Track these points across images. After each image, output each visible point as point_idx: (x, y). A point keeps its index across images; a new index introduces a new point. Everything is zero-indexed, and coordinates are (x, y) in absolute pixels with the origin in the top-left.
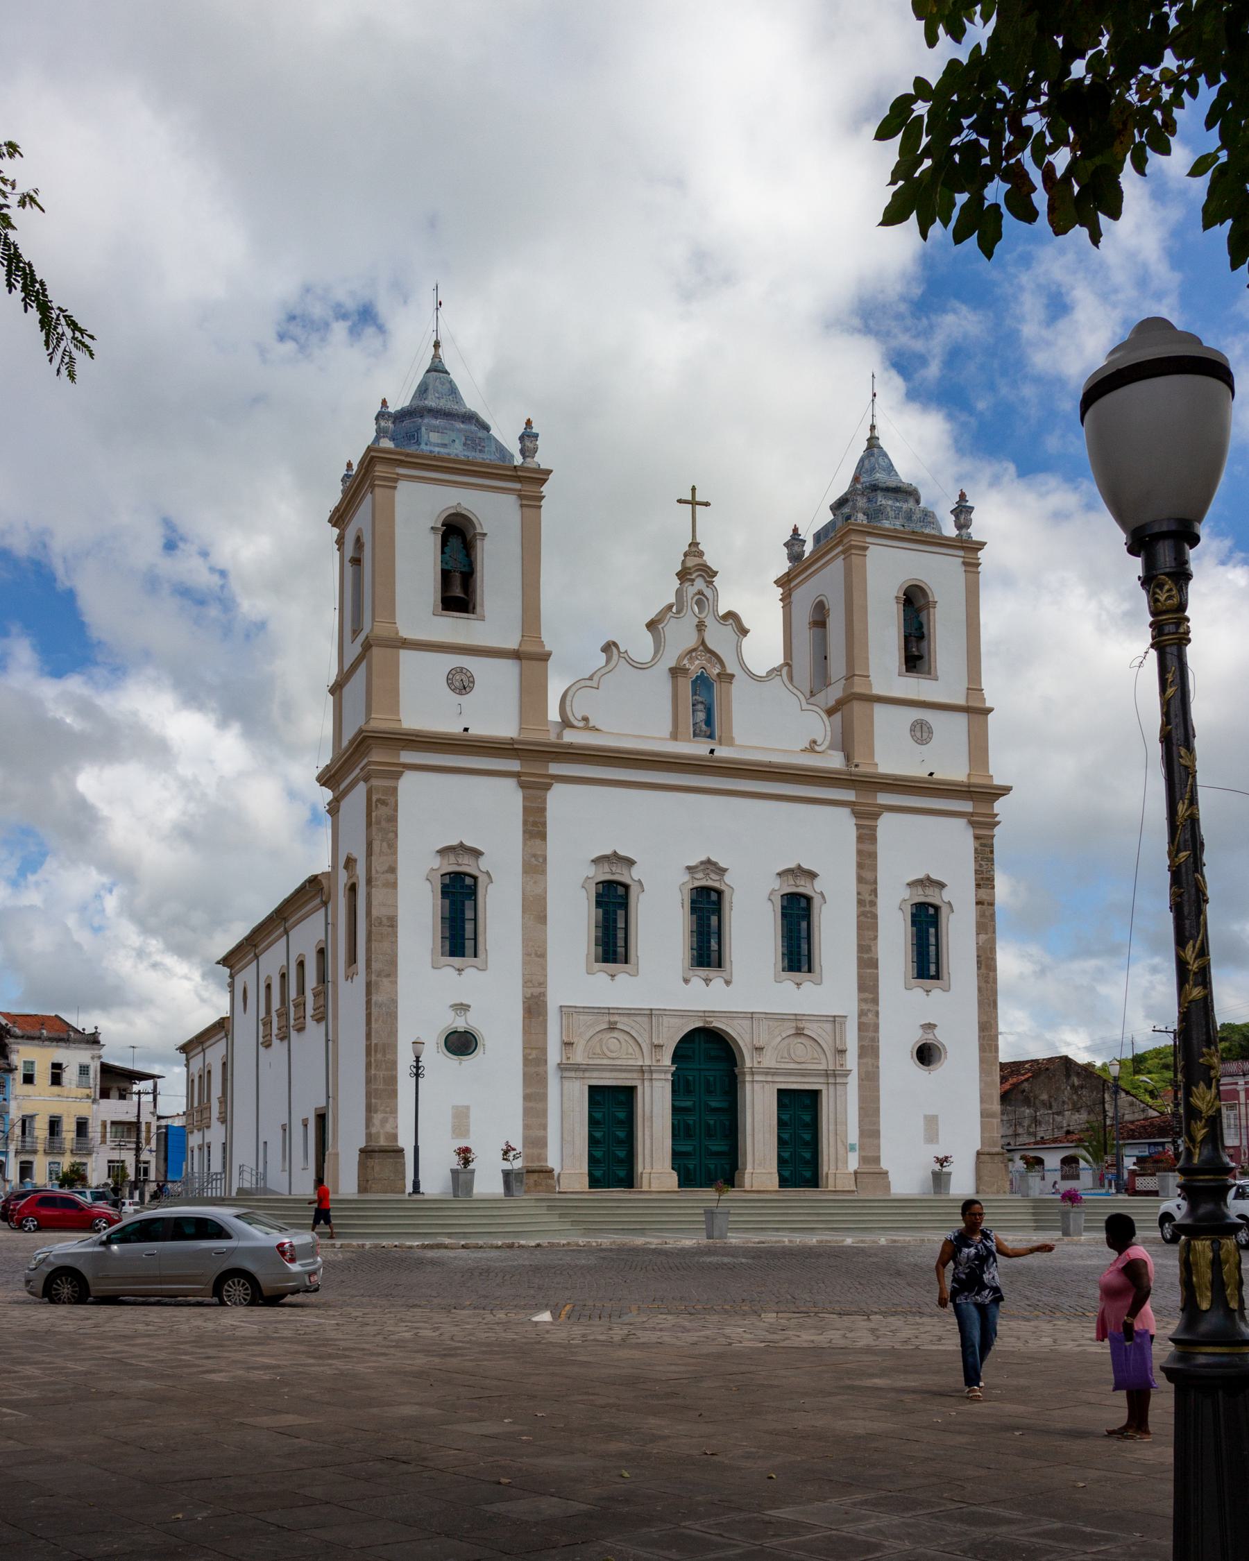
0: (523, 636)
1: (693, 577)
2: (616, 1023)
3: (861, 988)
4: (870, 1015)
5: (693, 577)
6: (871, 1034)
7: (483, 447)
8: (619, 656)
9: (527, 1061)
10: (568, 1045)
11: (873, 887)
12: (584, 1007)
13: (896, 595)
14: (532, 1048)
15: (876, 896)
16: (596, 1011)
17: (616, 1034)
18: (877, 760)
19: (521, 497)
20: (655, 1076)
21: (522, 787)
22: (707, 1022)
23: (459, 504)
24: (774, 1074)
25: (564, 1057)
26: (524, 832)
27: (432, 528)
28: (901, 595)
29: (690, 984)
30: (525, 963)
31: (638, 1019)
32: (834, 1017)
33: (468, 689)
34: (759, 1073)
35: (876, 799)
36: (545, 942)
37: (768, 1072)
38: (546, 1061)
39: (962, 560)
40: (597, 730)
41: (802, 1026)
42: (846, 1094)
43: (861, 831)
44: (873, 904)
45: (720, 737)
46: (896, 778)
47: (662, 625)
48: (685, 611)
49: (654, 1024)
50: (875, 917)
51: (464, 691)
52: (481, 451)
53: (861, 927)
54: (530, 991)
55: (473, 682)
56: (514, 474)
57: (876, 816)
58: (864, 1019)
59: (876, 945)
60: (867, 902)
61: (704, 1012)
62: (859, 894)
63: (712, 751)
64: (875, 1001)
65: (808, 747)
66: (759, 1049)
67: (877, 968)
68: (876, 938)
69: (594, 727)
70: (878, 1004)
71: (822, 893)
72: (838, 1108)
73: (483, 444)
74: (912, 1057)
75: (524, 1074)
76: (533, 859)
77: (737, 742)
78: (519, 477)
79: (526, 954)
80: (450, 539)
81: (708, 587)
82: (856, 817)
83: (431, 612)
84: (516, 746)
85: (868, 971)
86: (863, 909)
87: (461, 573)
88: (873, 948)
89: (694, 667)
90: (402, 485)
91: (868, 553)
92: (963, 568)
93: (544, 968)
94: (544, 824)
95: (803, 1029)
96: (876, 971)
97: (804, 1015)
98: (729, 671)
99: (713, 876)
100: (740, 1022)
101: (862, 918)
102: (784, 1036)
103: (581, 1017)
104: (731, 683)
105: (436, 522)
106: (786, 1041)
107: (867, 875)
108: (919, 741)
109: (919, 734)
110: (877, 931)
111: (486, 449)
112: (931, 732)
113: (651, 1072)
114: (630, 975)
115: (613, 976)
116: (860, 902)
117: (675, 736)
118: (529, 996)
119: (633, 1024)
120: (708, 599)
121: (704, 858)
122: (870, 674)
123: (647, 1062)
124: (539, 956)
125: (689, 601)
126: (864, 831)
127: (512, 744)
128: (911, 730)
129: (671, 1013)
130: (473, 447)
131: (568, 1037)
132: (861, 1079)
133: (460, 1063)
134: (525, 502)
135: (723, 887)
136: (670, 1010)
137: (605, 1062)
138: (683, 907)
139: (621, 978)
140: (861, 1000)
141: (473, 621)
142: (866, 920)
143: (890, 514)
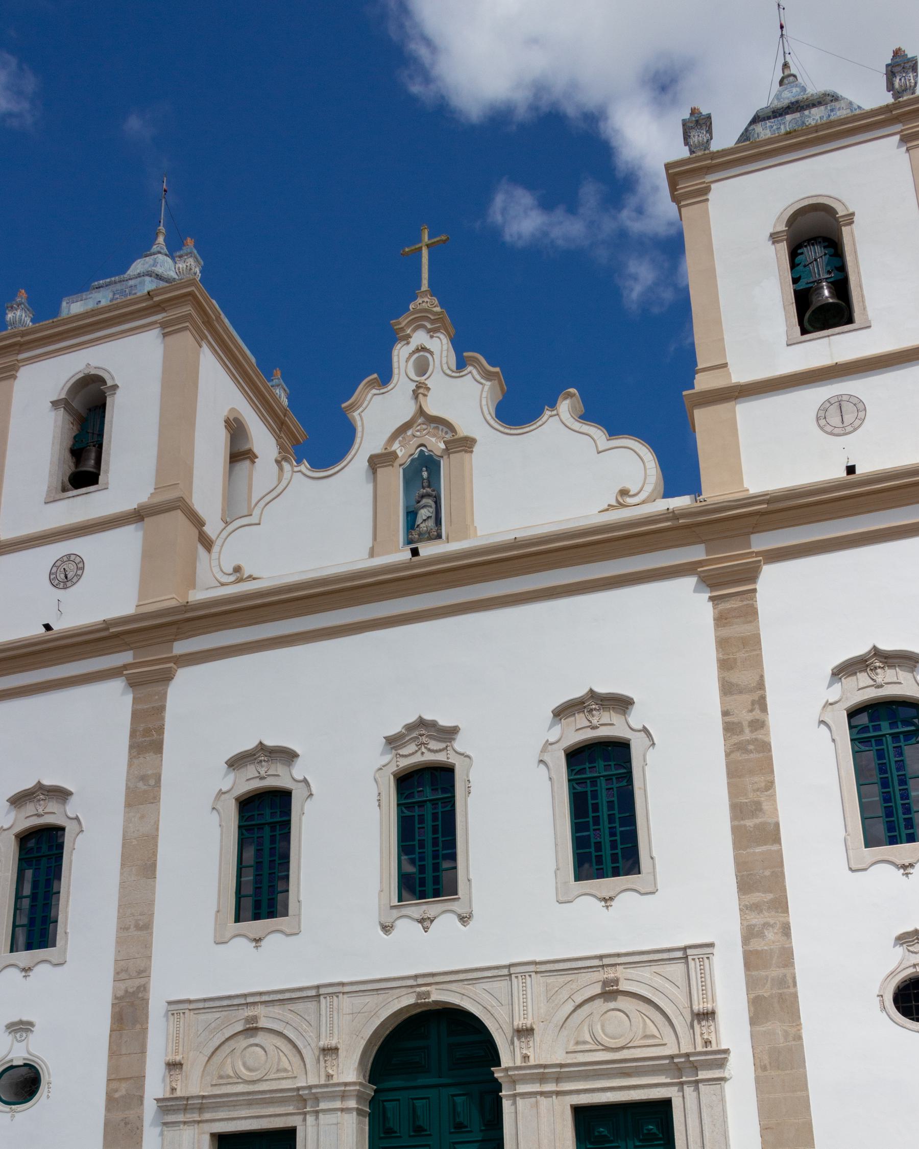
1: (408, 331)
2: (255, 1019)
3: (745, 884)
4: (770, 935)
5: (408, 331)
6: (775, 972)
9: (111, 1102)
10: (174, 1066)
11: (756, 696)
12: (205, 1000)
14: (120, 1080)
15: (764, 709)
16: (225, 1003)
17: (260, 1038)
18: (746, 485)
20: (323, 1105)
22: (419, 995)
24: (558, 1079)
25: (168, 1089)
26: (131, 747)
29: (394, 933)
30: (120, 942)
31: (299, 1007)
32: (685, 949)
34: (525, 1079)
36: (151, 903)
37: (542, 1073)
38: (141, 1098)
41: (612, 976)
42: (723, 1100)
44: (759, 725)
49: (323, 1012)
50: (765, 747)
51: (69, 584)
53: (734, 772)
54: (122, 986)
57: (750, 574)
58: (756, 945)
59: (773, 798)
60: (745, 724)
61: (416, 977)
62: (725, 713)
64: (781, 904)
65: (614, 503)
66: (525, 1032)
67: (777, 840)
68: (770, 785)
69: (250, 576)
70: (786, 910)
71: (645, 730)
72: (707, 1134)
73: (133, 292)
74: (884, 1008)
75: (107, 1124)
76: (141, 785)
79: (123, 928)
82: (708, 586)
85: (758, 850)
86: (736, 739)
88: (766, 806)
89: (404, 452)
93: (147, 945)
94: (161, 730)
95: (616, 981)
96: (775, 847)
97: (618, 955)
99: (434, 745)
100: (487, 986)
101: (737, 756)
102: (579, 999)
103: (202, 1017)
104: (472, 452)
105: (60, 394)
106: (586, 1008)
107: (744, 677)
110: (772, 772)
113: (317, 1099)
114: (288, 935)
115: (257, 941)
116: (730, 728)
118: (120, 993)
119: (289, 1016)
120: (431, 353)
121: (412, 719)
123: (312, 1081)
124: (138, 928)
127: (107, 629)
129: (355, 988)
131: (177, 1052)
132: (760, 1067)
133: (13, 1116)
134: (166, 330)
135: (453, 759)
136: (352, 984)
137: (241, 1088)
138: (379, 805)
139: (273, 942)
140: (745, 909)
142: (745, 757)
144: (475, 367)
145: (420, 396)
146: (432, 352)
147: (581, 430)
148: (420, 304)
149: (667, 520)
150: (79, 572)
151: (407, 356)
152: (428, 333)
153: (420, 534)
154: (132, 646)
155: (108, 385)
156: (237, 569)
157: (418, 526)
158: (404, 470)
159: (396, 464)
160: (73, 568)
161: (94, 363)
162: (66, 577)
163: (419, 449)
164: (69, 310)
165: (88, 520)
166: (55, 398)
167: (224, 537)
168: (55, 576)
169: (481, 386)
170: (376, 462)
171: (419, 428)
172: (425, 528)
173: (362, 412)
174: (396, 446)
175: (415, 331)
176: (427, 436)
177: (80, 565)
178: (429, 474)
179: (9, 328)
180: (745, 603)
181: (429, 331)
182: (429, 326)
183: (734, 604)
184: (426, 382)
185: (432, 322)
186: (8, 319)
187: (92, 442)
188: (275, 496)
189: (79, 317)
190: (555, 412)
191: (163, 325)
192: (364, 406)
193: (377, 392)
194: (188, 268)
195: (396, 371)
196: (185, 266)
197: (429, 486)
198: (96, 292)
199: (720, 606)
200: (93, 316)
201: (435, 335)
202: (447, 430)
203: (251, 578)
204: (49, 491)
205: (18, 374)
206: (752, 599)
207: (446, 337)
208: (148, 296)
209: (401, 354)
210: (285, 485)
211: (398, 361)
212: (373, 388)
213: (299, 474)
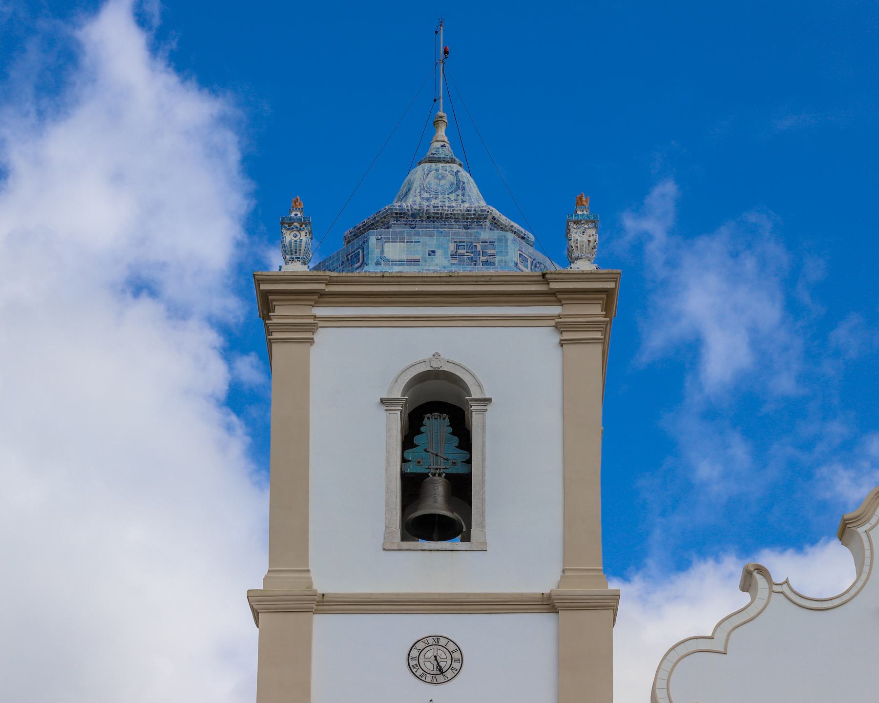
0: (563, 571)
7: (493, 255)
8: (772, 591)
19: (560, 328)
23: (436, 355)
27: (383, 401)
33: (449, 674)
51: (441, 678)
52: (485, 263)
55: (461, 661)
56: (542, 288)
73: (490, 252)
78: (554, 293)
80: (426, 421)
83: (381, 548)
87: (448, 477)
90: (323, 336)
111: (497, 258)
130: (471, 259)
155: (473, 397)
160: (443, 656)
161: (445, 356)
164: (382, 252)
165: (468, 594)
166: (385, 396)
168: (416, 662)
173: (870, 529)
177: (457, 657)
187: (437, 469)
194: (591, 245)
196: (586, 241)
200: (448, 283)
204: (388, 534)
208: (541, 278)
210: (760, 608)
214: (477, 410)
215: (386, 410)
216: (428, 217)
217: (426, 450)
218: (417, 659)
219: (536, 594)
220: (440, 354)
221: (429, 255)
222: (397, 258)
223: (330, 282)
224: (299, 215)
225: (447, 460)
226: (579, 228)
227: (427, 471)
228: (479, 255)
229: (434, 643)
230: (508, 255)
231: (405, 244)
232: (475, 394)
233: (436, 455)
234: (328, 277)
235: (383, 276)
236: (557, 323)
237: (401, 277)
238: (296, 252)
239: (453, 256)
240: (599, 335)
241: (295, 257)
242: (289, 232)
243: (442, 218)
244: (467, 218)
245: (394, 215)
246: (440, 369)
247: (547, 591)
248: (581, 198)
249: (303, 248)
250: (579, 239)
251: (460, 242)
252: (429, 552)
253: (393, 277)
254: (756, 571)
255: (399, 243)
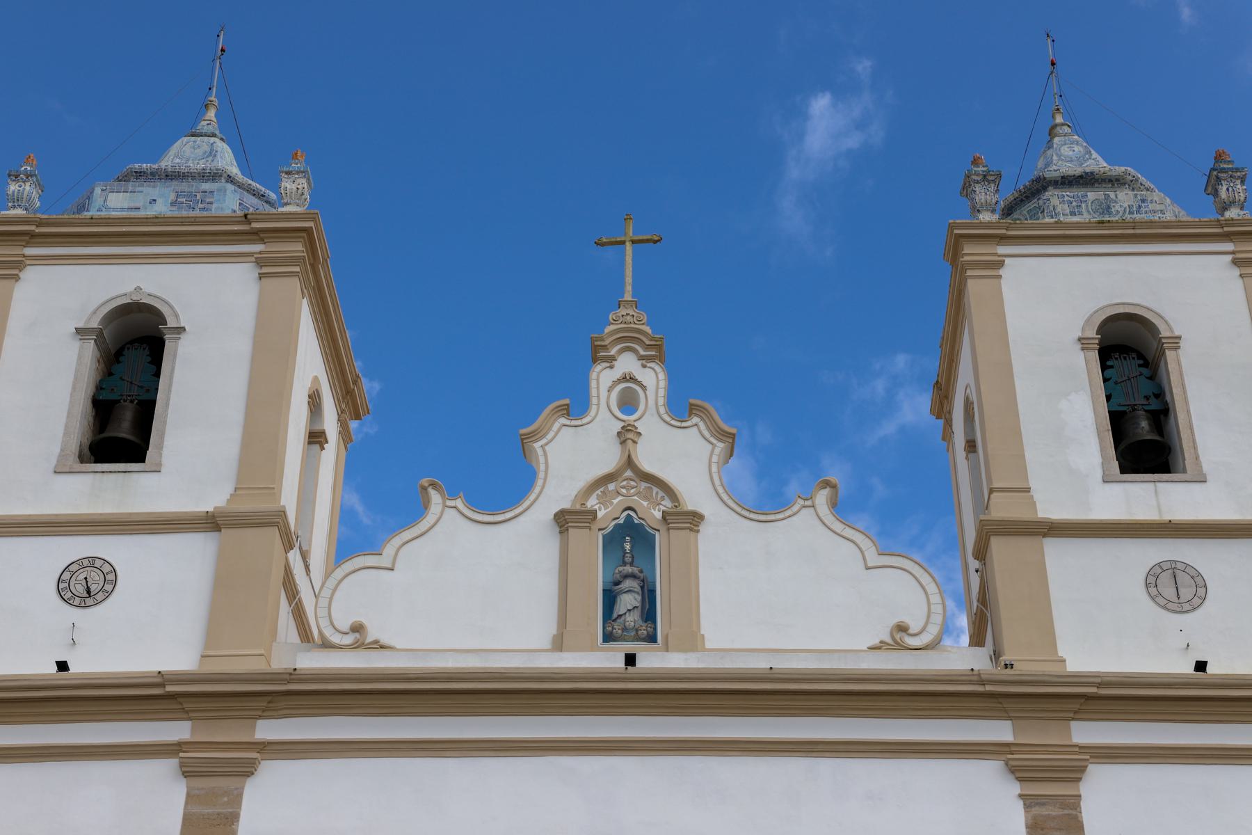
1: (613, 352)
5: (613, 352)
7: (211, 203)
13: (1080, 334)
18: (1061, 653)
21: (186, 774)
23: (138, 289)
27: (78, 331)
28: (1092, 333)
33: (100, 597)
35: (1071, 739)
39: (1229, 258)
40: (382, 647)
43: (1037, 810)
45: (666, 638)
46: (1104, 681)
47: (543, 441)
48: (593, 413)
51: (89, 601)
57: (1074, 773)
63: (630, 660)
65: (889, 640)
69: (376, 642)
73: (208, 200)
77: (708, 645)
81: (644, 366)
82: (1020, 780)
84: (170, 688)
89: (607, 512)
91: (1001, 272)
92: (1237, 272)
98: (690, 507)
104: (698, 531)
105: (89, 319)
108: (1170, 606)
109: (1169, 592)
111: (214, 206)
112: (1200, 583)
117: (559, 644)
120: (644, 388)
122: (1031, 485)
125: (604, 394)
126: (1045, 811)
127: (162, 685)
128: (1147, 585)
134: (265, 270)
141: (135, 476)
143: (1059, 209)
144: (702, 419)
145: (629, 442)
146: (645, 387)
147: (843, 534)
148: (623, 316)
149: (970, 682)
150: (108, 587)
151: (610, 384)
152: (639, 360)
153: (625, 629)
154: (191, 715)
156: (358, 628)
157: (620, 616)
158: (604, 536)
159: (595, 527)
161: (148, 288)
162: (89, 591)
163: (626, 513)
164: (105, 201)
165: (130, 514)
166: (81, 325)
167: (339, 577)
168: (67, 585)
169: (710, 447)
170: (564, 520)
171: (624, 483)
172: (633, 623)
173: (546, 444)
174: (592, 503)
175: (622, 353)
176: (636, 498)
177: (111, 578)
178: (632, 547)
179: (10, 204)
180: (1066, 812)
181: (641, 358)
182: (642, 352)
183: (1052, 810)
184: (636, 424)
185: (647, 348)
186: (10, 192)
187: (129, 396)
188: (416, 535)
189: (133, 221)
190: (809, 503)
191: (260, 262)
192: (549, 436)
193: (568, 422)
194: (300, 191)
195: (594, 400)
196: (295, 189)
197: (631, 564)
198: (149, 186)
199: (1033, 809)
200: (155, 224)
201: (648, 365)
202: (664, 495)
203: (379, 646)
204: (62, 456)
205: (22, 275)
206: (1076, 809)
207: (664, 371)
208: (243, 219)
209: (603, 380)
210: (432, 522)
211: (598, 388)
212: (562, 416)
213: (453, 511)
214: (170, 338)
215: (81, 339)
216: (167, 176)
217: (121, 379)
218: (68, 581)
219: (200, 512)
220: (142, 287)
221: (150, 203)
222: (119, 205)
223: (40, 223)
224: (29, 169)
225: (142, 387)
226: (290, 178)
227: (119, 398)
228: (198, 202)
229: (89, 565)
230: (225, 202)
231: (128, 194)
232: (171, 323)
233: (131, 383)
234: (38, 220)
235: (92, 218)
236: (256, 258)
237: (109, 218)
238: (18, 200)
239: (172, 204)
240: (297, 269)
241: (16, 204)
242: (14, 183)
243: (179, 176)
244: (203, 177)
245: (134, 174)
246: (141, 301)
247: (211, 509)
248: (296, 154)
249: (25, 196)
250: (288, 187)
251: (181, 192)
252: (101, 474)
253: (101, 218)
254: (431, 487)
255: (122, 193)
